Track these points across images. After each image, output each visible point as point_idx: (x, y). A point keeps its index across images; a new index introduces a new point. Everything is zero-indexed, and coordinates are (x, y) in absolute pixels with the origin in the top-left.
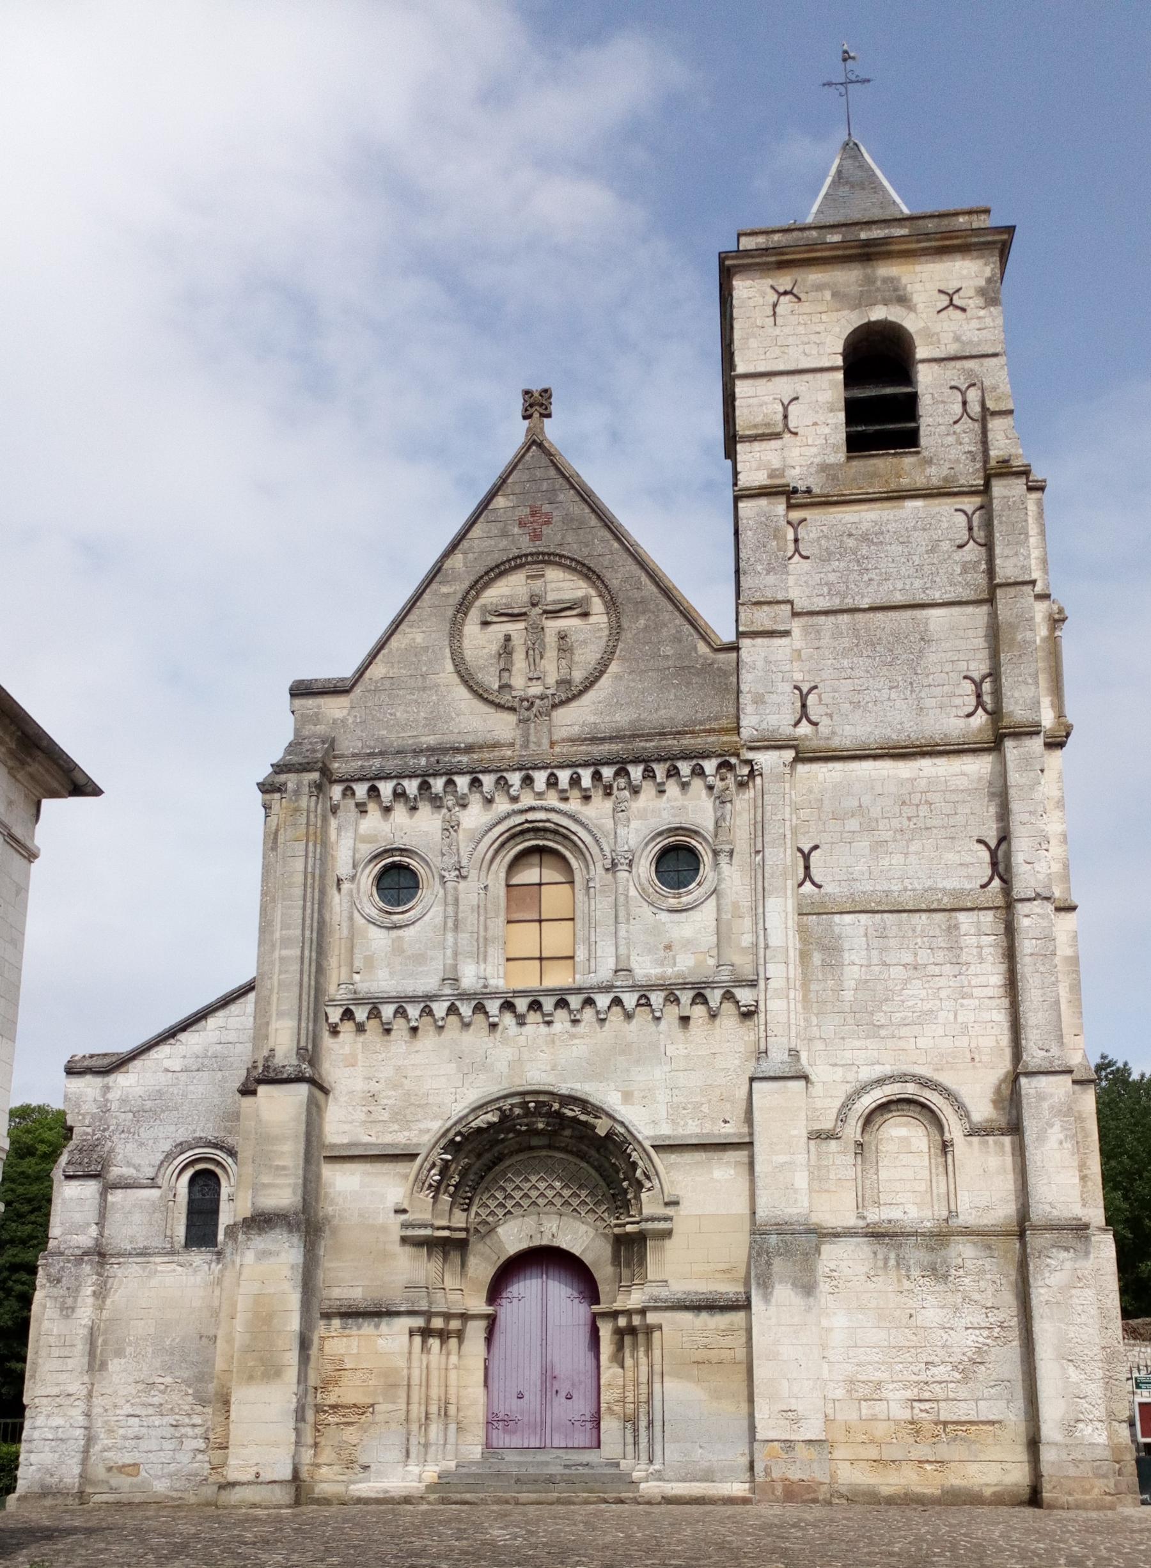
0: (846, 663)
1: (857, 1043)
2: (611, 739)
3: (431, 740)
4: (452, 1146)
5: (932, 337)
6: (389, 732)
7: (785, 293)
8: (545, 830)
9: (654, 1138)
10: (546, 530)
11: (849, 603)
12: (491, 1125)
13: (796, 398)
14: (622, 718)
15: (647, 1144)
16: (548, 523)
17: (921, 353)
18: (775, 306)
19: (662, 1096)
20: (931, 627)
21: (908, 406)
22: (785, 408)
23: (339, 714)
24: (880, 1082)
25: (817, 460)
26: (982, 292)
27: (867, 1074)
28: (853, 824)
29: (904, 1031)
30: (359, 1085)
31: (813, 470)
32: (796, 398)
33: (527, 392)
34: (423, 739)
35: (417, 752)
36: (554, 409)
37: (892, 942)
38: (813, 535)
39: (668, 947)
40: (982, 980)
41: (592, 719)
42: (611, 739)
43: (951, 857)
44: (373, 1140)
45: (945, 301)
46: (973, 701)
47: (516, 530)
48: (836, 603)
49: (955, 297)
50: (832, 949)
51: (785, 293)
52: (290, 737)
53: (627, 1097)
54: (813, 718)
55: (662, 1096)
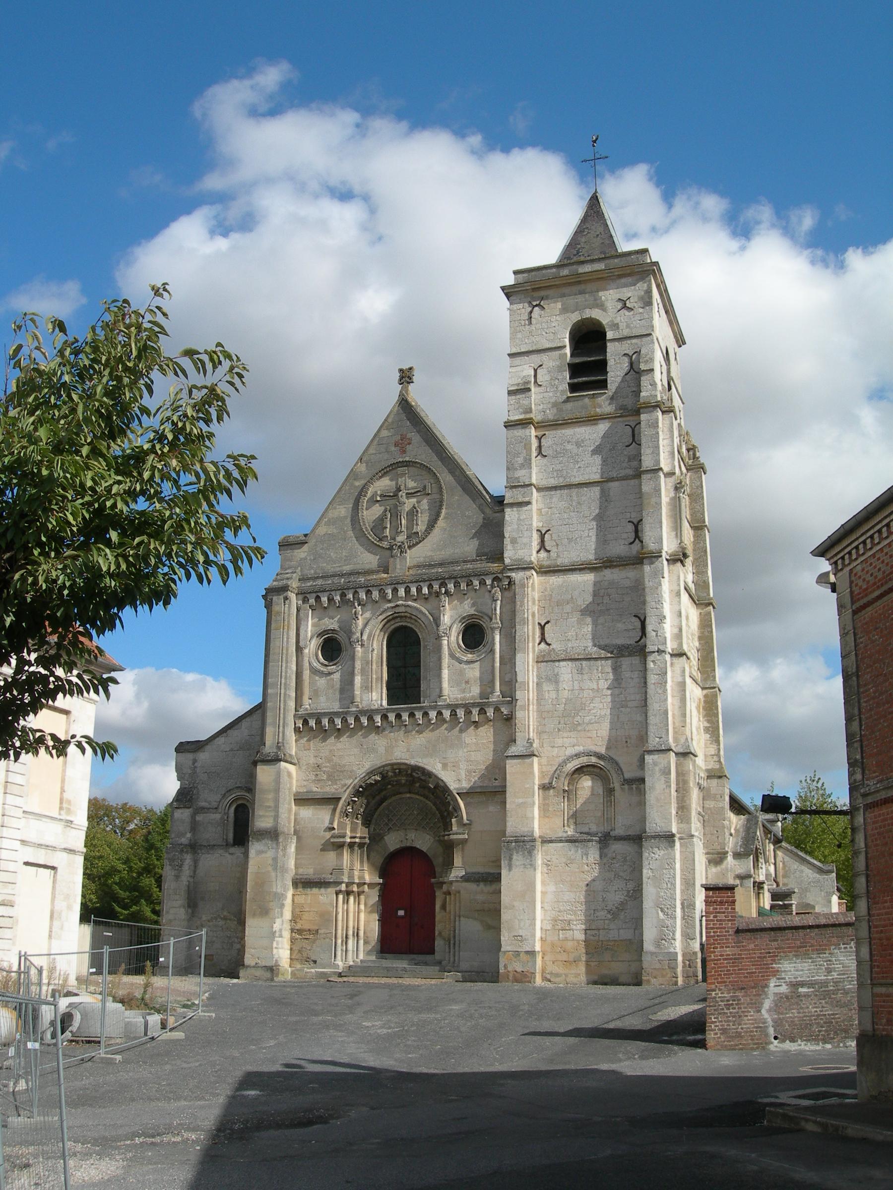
0: (566, 516)
1: (565, 735)
2: (441, 565)
3: (347, 568)
4: (357, 793)
5: (616, 326)
6: (328, 564)
7: (536, 306)
8: (406, 617)
9: (457, 789)
10: (409, 448)
11: (569, 481)
12: (377, 782)
13: (541, 366)
14: (446, 554)
15: (455, 792)
16: (409, 444)
17: (610, 335)
18: (531, 312)
19: (463, 766)
20: (611, 494)
21: (601, 366)
22: (535, 371)
23: (303, 555)
24: (577, 755)
25: (553, 400)
26: (641, 298)
27: (570, 751)
28: (568, 608)
29: (590, 727)
30: (312, 761)
31: (550, 406)
32: (541, 366)
33: (401, 370)
34: (344, 568)
35: (342, 575)
36: (414, 379)
37: (586, 677)
38: (550, 443)
39: (467, 682)
40: (633, 697)
41: (429, 554)
42: (441, 565)
43: (620, 626)
44: (319, 790)
45: (620, 305)
46: (633, 534)
47: (393, 448)
48: (561, 481)
49: (627, 302)
50: (555, 679)
51: (536, 306)
52: (278, 570)
53: (445, 766)
54: (548, 548)
55: (463, 766)
